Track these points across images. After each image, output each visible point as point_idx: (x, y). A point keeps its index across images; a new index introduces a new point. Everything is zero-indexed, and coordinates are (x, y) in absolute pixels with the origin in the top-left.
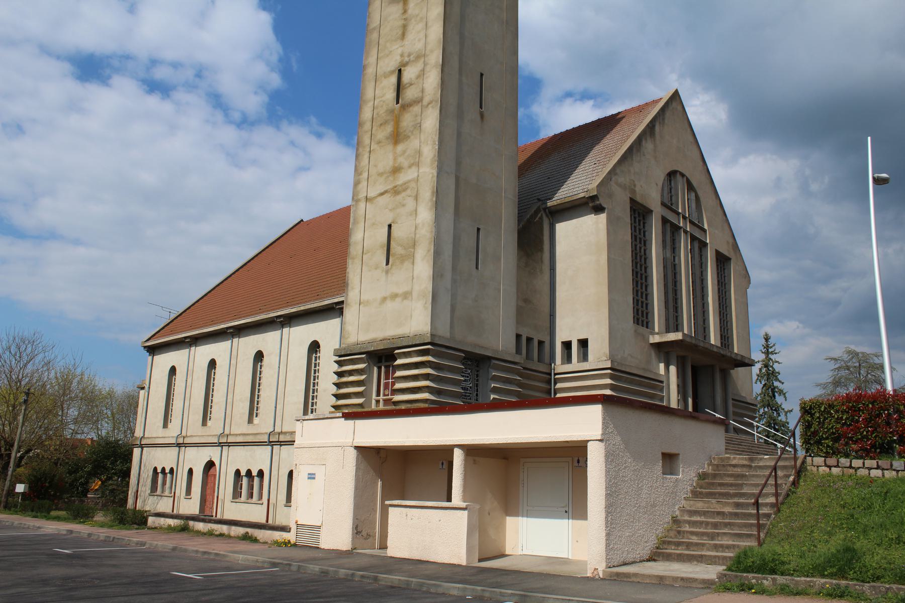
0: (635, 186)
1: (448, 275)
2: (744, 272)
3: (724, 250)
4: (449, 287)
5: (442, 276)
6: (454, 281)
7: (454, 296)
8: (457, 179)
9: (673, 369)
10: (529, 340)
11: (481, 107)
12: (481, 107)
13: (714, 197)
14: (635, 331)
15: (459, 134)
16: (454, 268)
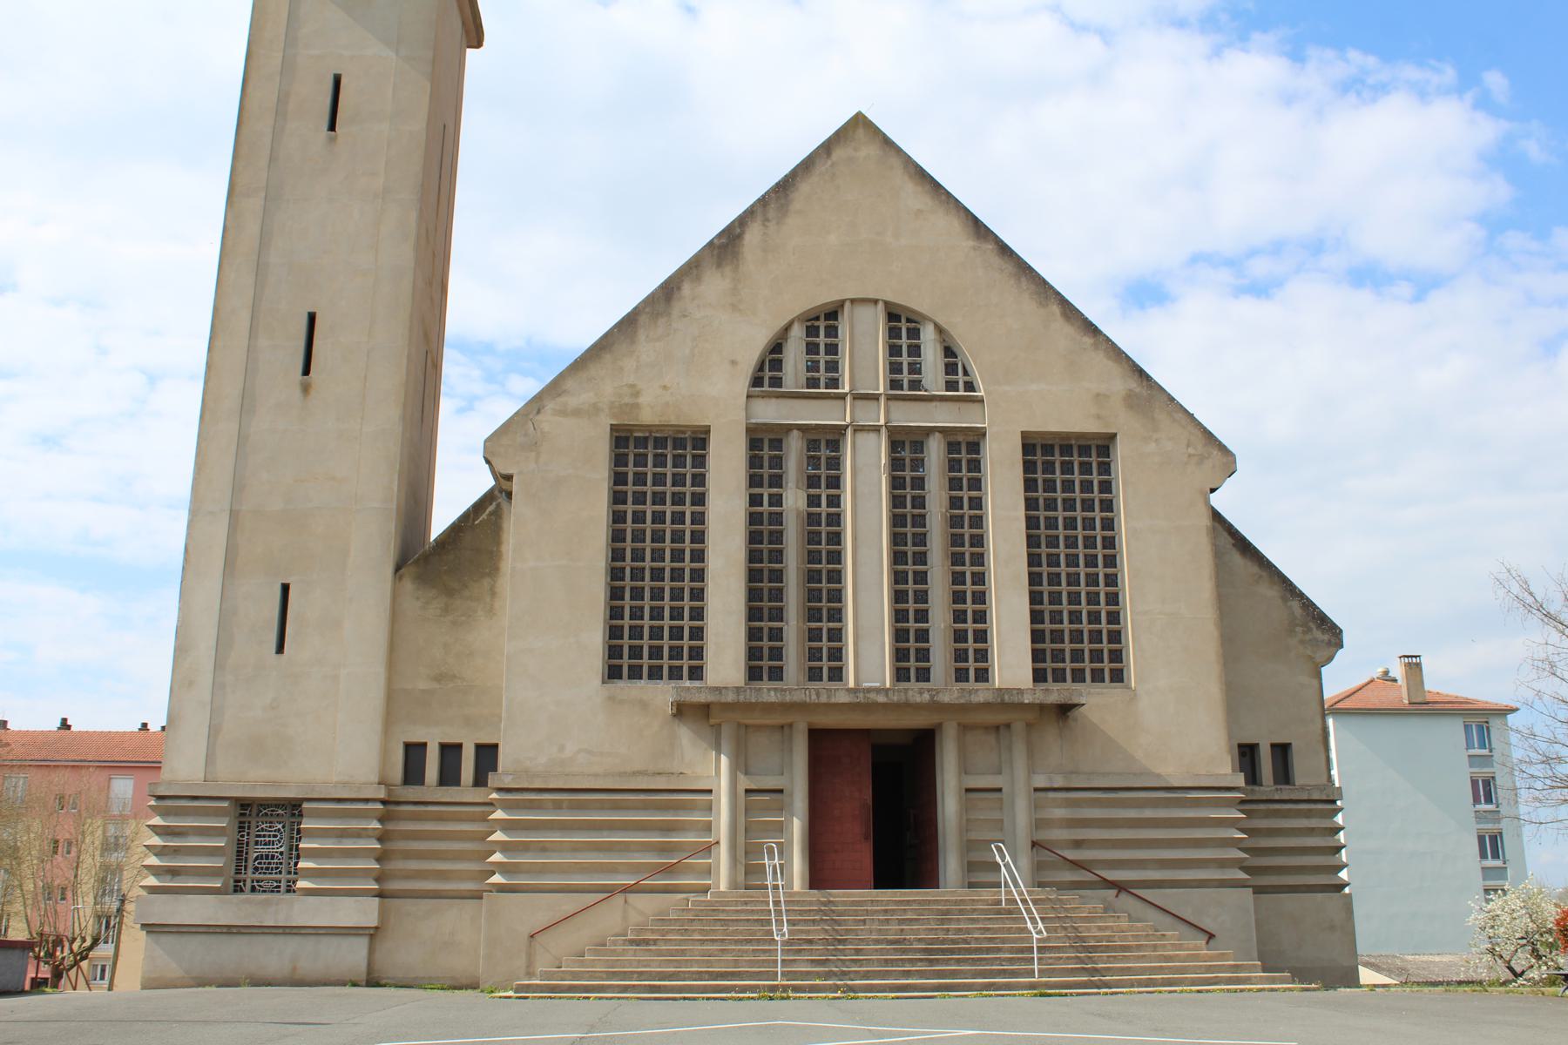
0: (637, 394)
1: (206, 679)
2: (1199, 446)
3: (1076, 420)
4: (206, 695)
5: (191, 683)
6: (217, 687)
7: (216, 712)
8: (234, 516)
9: (724, 759)
10: (450, 752)
11: (306, 371)
12: (306, 371)
13: (1027, 303)
14: (611, 698)
15: (242, 439)
16: (219, 666)
